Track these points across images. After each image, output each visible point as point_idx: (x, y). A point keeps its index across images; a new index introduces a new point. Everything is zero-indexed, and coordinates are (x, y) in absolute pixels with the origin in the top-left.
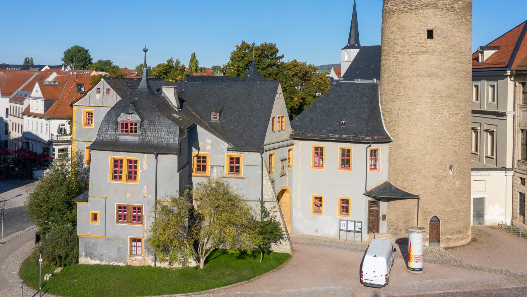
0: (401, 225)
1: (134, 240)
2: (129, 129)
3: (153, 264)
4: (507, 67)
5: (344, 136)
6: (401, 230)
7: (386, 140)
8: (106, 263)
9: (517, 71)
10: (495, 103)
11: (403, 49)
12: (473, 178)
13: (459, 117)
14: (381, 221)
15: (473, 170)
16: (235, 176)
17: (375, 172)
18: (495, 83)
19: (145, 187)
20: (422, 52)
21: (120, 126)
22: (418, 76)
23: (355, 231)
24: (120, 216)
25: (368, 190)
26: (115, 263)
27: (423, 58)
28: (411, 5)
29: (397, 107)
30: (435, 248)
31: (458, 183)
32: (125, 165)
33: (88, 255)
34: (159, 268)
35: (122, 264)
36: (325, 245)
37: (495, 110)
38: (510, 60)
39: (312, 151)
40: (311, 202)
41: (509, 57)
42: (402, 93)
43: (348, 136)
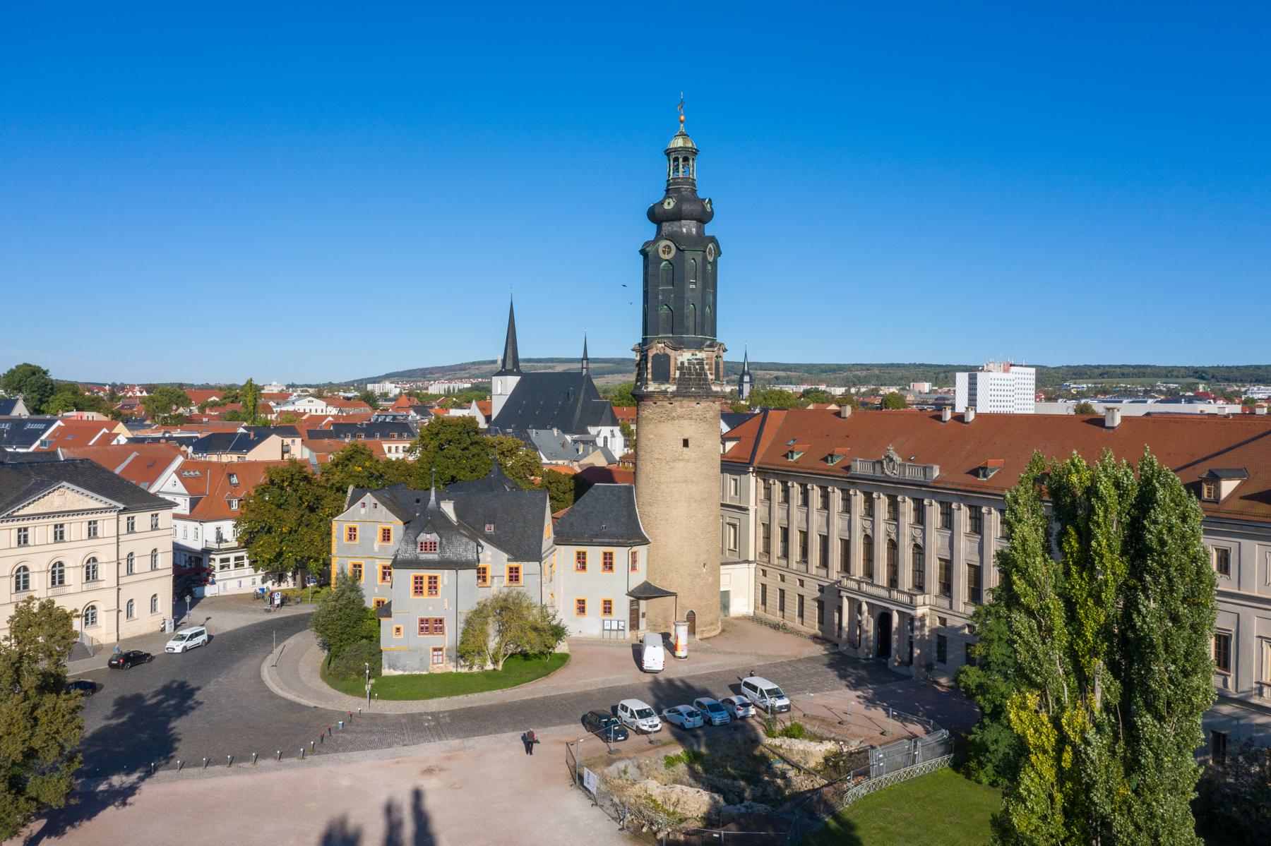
1: (435, 650)
2: (428, 548)
3: (454, 670)
4: (749, 463)
5: (607, 540)
7: (645, 542)
8: (409, 673)
9: (758, 468)
11: (660, 456)
12: (722, 572)
13: (711, 518)
14: (641, 619)
15: (722, 564)
16: (514, 585)
17: (635, 572)
18: (738, 477)
19: (446, 600)
20: (679, 460)
21: (419, 545)
22: (675, 482)
23: (618, 630)
24: (422, 628)
26: (418, 673)
27: (679, 465)
29: (655, 511)
30: (693, 640)
31: (710, 579)
32: (426, 581)
33: (391, 667)
34: (460, 673)
35: (424, 673)
36: (593, 645)
37: (737, 504)
39: (575, 556)
40: (574, 605)
42: (660, 498)
43: (611, 540)
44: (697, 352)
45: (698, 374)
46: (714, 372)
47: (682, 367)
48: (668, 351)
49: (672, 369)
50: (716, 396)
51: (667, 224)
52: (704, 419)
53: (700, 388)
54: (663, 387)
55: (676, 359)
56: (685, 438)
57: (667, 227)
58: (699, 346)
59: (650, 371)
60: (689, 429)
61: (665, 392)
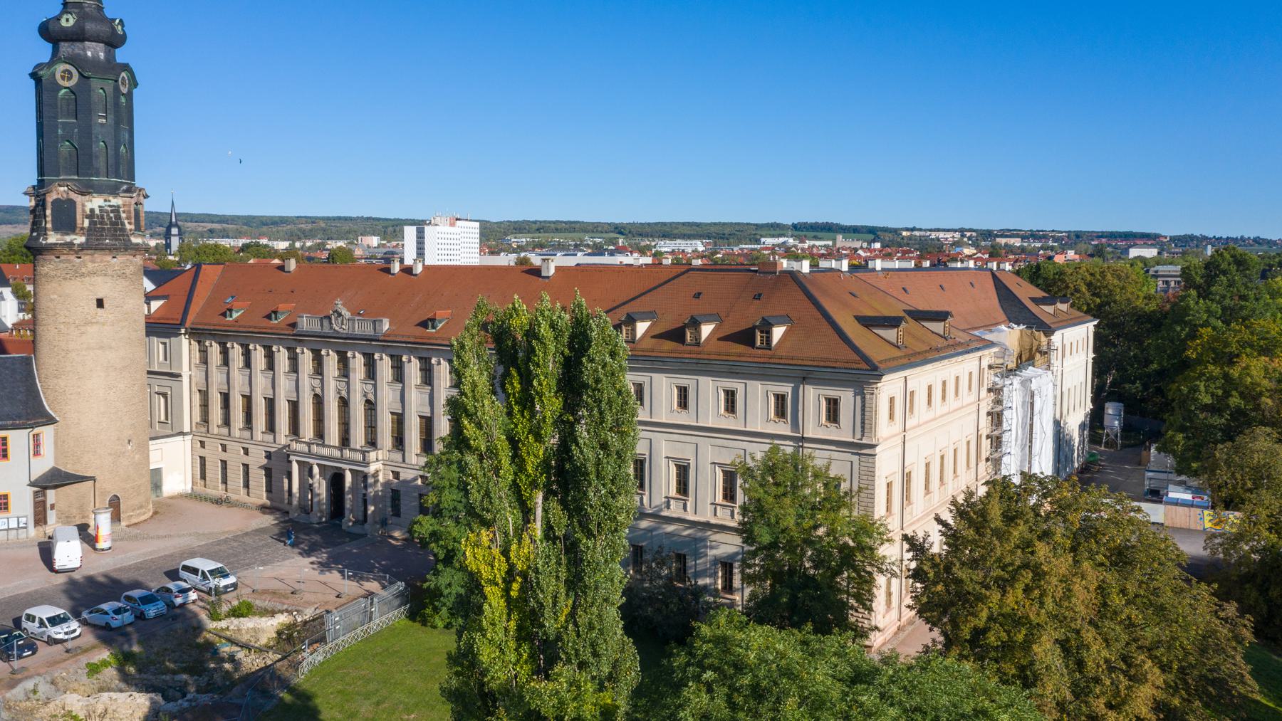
0: (74, 511)
4: (180, 324)
6: (75, 517)
7: (51, 421)
9: (192, 329)
10: (168, 362)
11: (67, 320)
13: (136, 388)
14: (49, 512)
17: (38, 458)
18: (167, 341)
20: (92, 323)
25: (32, 480)
27: (92, 329)
28: (76, 271)
29: (62, 384)
37: (168, 371)
38: (183, 315)
41: (182, 312)
44: (111, 198)
45: (112, 224)
46: (133, 221)
47: (91, 215)
48: (73, 196)
49: (79, 217)
50: (137, 249)
51: (66, 44)
52: (123, 276)
53: (116, 240)
54: (68, 238)
55: (83, 205)
56: (100, 296)
57: (65, 48)
58: (114, 191)
59: (49, 219)
60: (103, 287)
61: (71, 244)
